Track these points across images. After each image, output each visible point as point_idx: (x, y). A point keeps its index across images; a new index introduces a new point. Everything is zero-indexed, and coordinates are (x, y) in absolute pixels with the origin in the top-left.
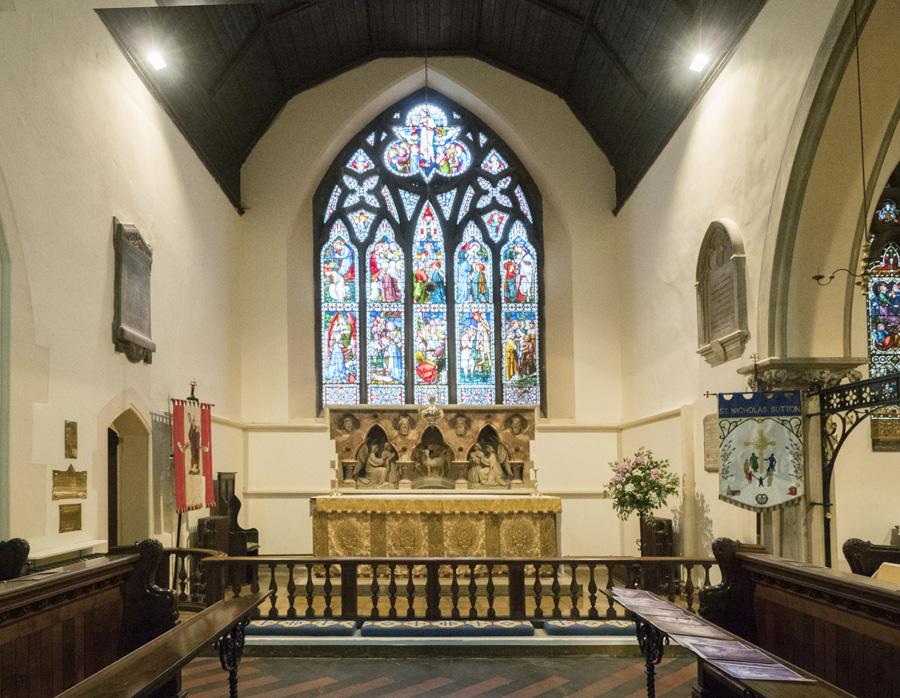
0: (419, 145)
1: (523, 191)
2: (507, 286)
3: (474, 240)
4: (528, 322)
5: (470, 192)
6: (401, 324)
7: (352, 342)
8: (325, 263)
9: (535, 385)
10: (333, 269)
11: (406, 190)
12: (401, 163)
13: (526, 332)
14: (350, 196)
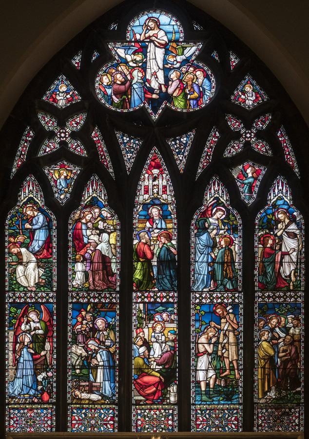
0: (144, 68)
1: (288, 134)
2: (264, 273)
4: (290, 317)
5: (214, 137)
6: (114, 320)
7: (48, 346)
8: (11, 235)
9: (298, 405)
10: (22, 245)
11: (125, 132)
12: (117, 93)
13: (286, 330)
14: (46, 142)
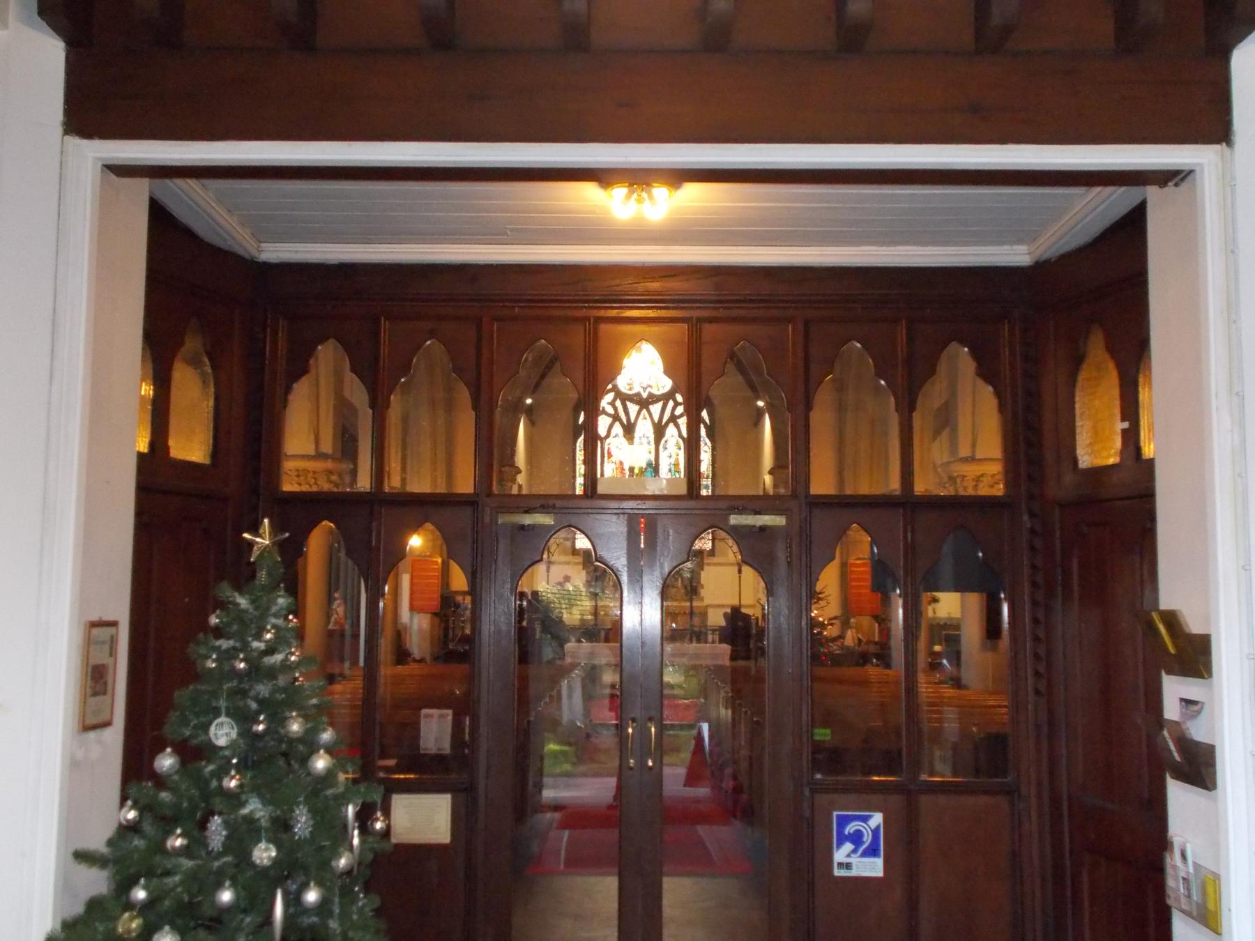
3: (673, 436)
5: (671, 403)
